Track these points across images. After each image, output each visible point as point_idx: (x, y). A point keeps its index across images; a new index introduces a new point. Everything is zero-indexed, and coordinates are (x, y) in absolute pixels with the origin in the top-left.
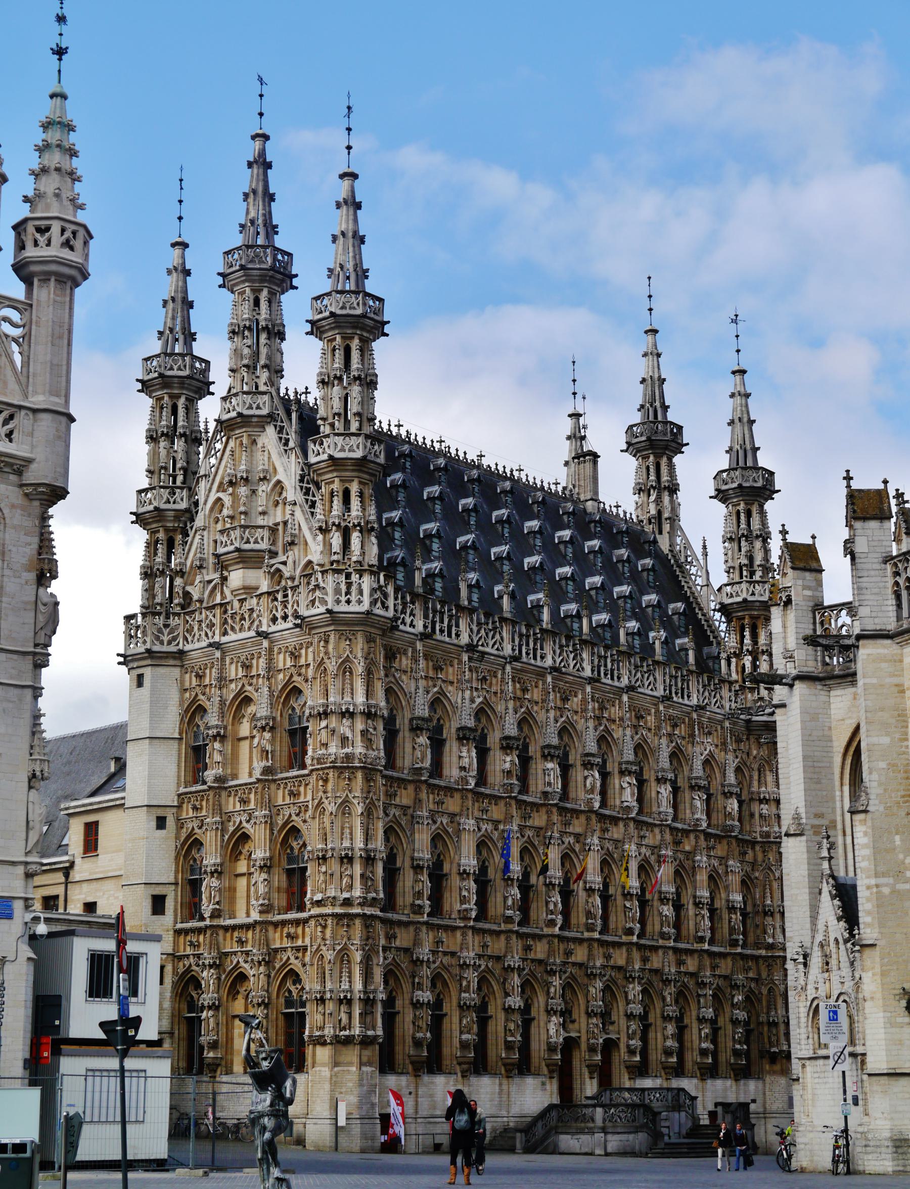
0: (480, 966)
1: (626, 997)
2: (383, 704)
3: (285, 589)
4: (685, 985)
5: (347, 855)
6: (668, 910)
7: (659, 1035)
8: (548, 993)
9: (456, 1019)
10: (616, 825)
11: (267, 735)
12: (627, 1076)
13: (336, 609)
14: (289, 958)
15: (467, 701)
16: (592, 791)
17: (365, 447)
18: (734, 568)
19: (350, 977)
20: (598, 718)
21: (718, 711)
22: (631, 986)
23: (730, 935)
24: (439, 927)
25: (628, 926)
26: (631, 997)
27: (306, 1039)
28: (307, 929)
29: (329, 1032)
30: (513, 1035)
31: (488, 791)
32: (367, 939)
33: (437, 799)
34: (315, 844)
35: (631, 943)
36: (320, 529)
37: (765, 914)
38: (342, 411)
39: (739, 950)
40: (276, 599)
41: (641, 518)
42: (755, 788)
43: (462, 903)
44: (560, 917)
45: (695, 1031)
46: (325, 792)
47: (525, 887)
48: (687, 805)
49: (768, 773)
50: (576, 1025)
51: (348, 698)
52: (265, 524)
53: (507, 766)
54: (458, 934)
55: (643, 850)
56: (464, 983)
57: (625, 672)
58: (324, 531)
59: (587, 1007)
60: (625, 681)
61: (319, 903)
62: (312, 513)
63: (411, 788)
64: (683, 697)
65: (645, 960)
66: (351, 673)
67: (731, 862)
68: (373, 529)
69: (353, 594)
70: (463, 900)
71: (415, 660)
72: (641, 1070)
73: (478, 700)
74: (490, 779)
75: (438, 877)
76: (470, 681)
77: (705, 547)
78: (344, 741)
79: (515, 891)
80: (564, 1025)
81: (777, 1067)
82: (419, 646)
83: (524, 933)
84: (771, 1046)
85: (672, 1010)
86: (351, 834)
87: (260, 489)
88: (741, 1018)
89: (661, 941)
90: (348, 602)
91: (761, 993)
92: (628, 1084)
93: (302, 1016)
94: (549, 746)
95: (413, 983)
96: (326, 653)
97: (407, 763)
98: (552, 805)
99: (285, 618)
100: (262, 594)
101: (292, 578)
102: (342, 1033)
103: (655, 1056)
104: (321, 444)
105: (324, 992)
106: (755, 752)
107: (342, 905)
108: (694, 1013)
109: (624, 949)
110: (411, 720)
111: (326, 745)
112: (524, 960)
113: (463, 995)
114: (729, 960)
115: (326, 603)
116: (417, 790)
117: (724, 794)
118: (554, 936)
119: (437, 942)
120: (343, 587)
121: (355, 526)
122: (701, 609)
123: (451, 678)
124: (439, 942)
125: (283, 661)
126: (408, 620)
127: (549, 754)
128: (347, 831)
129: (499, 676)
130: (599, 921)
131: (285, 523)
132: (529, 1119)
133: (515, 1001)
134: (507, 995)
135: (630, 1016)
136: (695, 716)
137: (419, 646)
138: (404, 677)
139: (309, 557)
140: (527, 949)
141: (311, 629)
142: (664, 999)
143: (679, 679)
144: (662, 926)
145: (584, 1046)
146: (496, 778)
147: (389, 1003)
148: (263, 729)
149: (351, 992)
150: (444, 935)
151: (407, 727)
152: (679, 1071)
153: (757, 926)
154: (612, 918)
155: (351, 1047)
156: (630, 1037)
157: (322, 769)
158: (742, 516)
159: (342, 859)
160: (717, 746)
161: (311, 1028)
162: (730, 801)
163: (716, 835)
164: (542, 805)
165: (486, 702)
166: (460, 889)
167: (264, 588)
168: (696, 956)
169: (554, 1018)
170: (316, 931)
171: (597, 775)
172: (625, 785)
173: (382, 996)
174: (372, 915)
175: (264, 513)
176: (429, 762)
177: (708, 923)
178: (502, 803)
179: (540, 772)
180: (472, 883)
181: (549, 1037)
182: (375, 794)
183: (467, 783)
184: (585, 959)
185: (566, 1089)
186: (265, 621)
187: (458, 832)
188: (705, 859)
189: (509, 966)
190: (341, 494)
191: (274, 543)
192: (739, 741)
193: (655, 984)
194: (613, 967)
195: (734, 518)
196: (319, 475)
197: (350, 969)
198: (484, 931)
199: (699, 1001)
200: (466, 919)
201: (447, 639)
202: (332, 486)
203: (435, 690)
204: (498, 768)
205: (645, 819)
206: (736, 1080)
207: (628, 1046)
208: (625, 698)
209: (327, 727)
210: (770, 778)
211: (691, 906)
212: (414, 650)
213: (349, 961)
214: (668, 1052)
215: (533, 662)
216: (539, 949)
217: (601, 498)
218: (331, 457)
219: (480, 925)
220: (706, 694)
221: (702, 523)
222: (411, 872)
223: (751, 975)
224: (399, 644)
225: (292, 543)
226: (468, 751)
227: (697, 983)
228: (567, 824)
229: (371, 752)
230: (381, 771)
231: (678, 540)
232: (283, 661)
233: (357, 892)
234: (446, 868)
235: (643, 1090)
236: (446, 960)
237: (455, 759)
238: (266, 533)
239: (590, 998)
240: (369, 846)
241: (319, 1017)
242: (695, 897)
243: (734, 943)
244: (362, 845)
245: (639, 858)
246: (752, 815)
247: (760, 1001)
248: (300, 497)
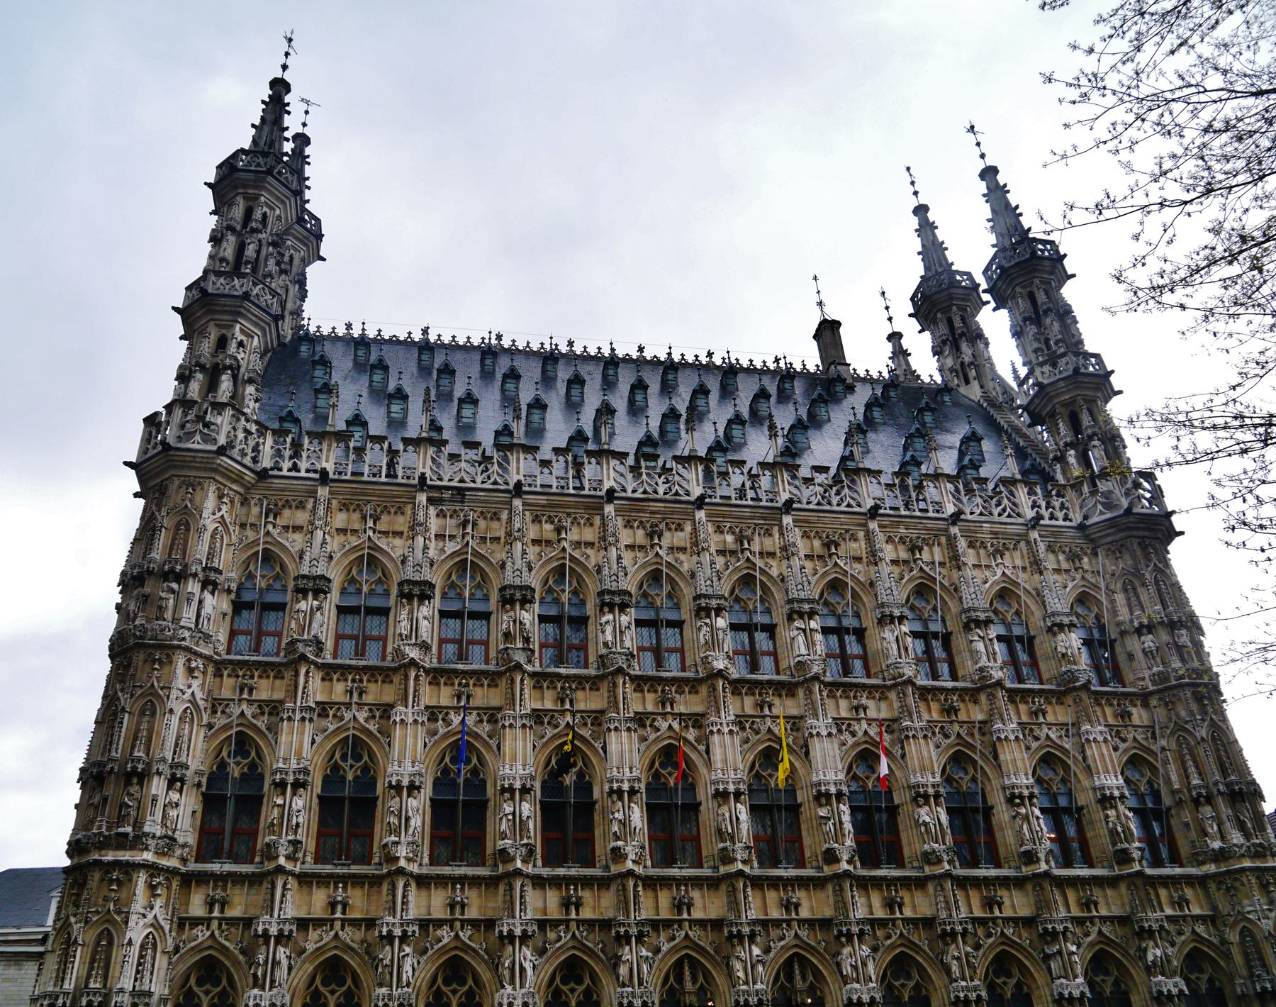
1: (841, 973)
10: (793, 695)
22: (847, 950)
23: (1114, 844)
37: (1196, 802)
39: (1137, 867)
89: (927, 869)
91: (1224, 942)
142: (948, 970)
153: (1187, 825)
168: (1029, 887)
174: (117, 864)
246: (1131, 656)
247: (1228, 956)
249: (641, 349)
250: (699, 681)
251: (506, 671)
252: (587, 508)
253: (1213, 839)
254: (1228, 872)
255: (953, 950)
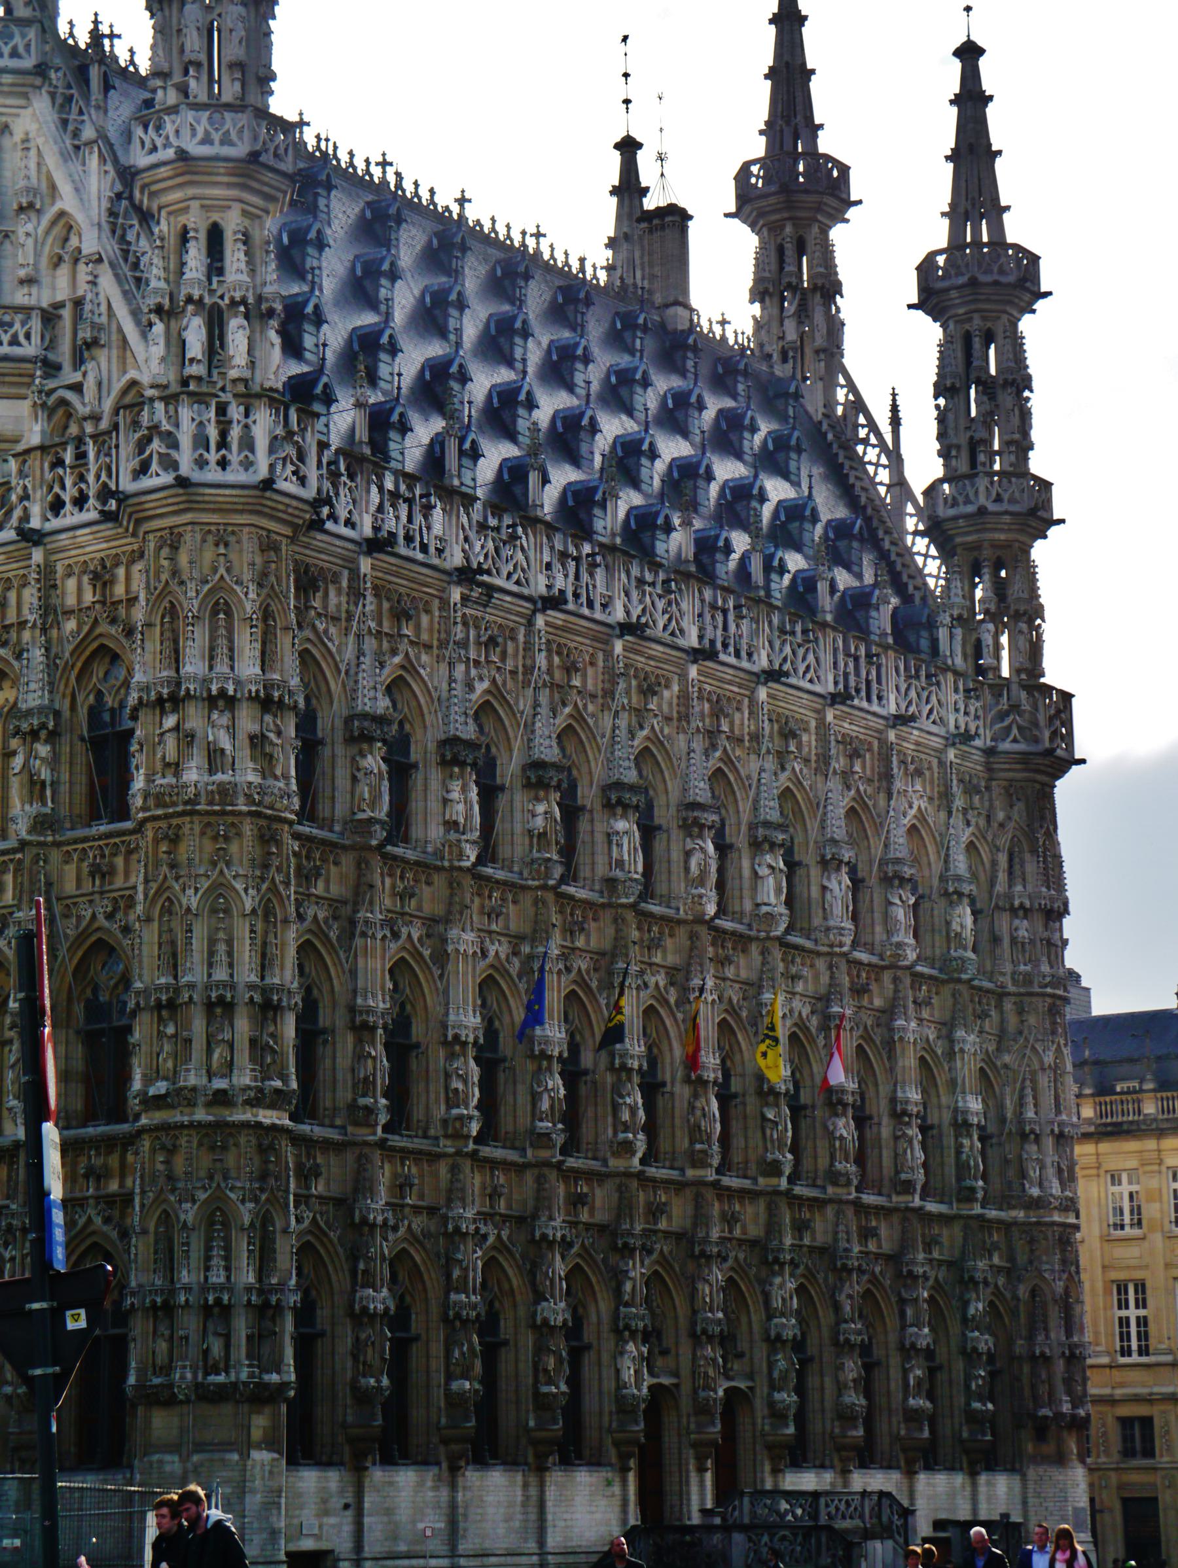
0: (485, 1237)
2: (295, 682)
3: (80, 441)
4: (874, 1280)
5: (221, 998)
6: (845, 1127)
7: (828, 1381)
8: (618, 1291)
9: (437, 1349)
11: (43, 750)
12: (767, 1468)
13: (197, 476)
14: (90, 1220)
15: (459, 689)
16: (701, 881)
17: (255, 138)
18: (958, 447)
19: (227, 1258)
20: (712, 735)
21: (934, 729)
22: (778, 1280)
23: (959, 1179)
24: (405, 1153)
25: (770, 1157)
26: (777, 1303)
27: (129, 1391)
28: (130, 1158)
29: (184, 1375)
30: (550, 1382)
31: (500, 875)
32: (263, 1176)
33: (400, 886)
34: (148, 975)
35: (777, 1193)
36: (159, 310)
37: (1024, 1136)
38: (203, 57)
39: (977, 1210)
40: (60, 463)
41: (768, 349)
42: (1001, 887)
43: (449, 1107)
44: (641, 1136)
45: (895, 1374)
46: (173, 866)
47: (573, 1075)
48: (878, 916)
49: (1027, 856)
50: (670, 1361)
51: (222, 668)
52: (33, 302)
53: (539, 822)
54: (443, 1169)
55: (797, 1004)
56: (456, 1273)
57: (762, 643)
58: (167, 313)
59: (693, 1324)
60: (762, 661)
61: (159, 1102)
62: (138, 280)
63: (348, 861)
64: (869, 700)
65: (800, 1227)
66: (229, 614)
67: (960, 1033)
68: (271, 313)
69: (235, 447)
70: (453, 1099)
71: (356, 594)
72: (797, 1455)
73: (481, 687)
74: (504, 851)
75: (401, 1048)
76: (464, 644)
77: (895, 409)
78: (215, 758)
79: (556, 1083)
80: (649, 1361)
81: (1049, 1448)
82: (365, 565)
83: (572, 1170)
84: (1038, 1405)
85: (854, 1329)
86: (230, 954)
87: (21, 231)
88: (982, 1348)
89: (830, 1190)
90: (223, 464)
92: (768, 1486)
93: (120, 1346)
94: (618, 785)
95: (354, 1272)
96: (175, 573)
97: (341, 810)
98: (623, 906)
99: (80, 501)
100: (28, 452)
101: (96, 418)
102: (212, 1378)
103: (821, 1424)
104: (158, 128)
105: (173, 1292)
106: (1001, 816)
107: (209, 1105)
108: (893, 1338)
109: (762, 1204)
110: (349, 720)
111: (176, 768)
112: (573, 1224)
113: (453, 1297)
114: (957, 1229)
115: (175, 466)
116: (361, 865)
117: (946, 894)
118: (628, 1175)
119: (401, 1186)
120: (213, 433)
121: (234, 303)
122: (888, 532)
123: (425, 637)
124: (401, 1186)
125: (74, 591)
126: (343, 514)
127: (619, 802)
128: (222, 948)
129: (521, 638)
130: (716, 1147)
131: (78, 303)
132: (594, 1559)
133: (556, 1311)
134: (539, 1297)
135: (775, 1342)
136: (892, 736)
137: (365, 565)
138: (332, 630)
139: (132, 374)
140: (577, 1201)
141: (138, 522)
142: (837, 1307)
143: (862, 660)
144: (833, 1158)
145: (685, 1403)
146: (514, 847)
147: (305, 1314)
148: (34, 734)
149: (231, 1290)
150: (414, 1170)
151: (339, 736)
152: (867, 1457)
153: (1007, 1161)
154: (738, 1142)
155: (227, 1409)
156: (773, 1387)
157: (167, 817)
158: (977, 343)
159: (210, 1006)
160: (931, 799)
161: (142, 1372)
162: (959, 910)
163: (931, 977)
164: (603, 905)
165: (496, 690)
166: (447, 1076)
167: (36, 440)
168: (896, 1219)
169: (631, 1347)
170: (153, 1161)
171: (711, 848)
172: (763, 871)
173: (294, 1299)
174: (274, 1127)
175: (29, 281)
176: (386, 807)
177: (920, 1155)
178: (527, 900)
179: (600, 838)
180: (472, 1063)
181: (620, 1385)
182: (279, 870)
183: (461, 855)
184: (688, 1223)
185: (654, 1497)
186: (36, 510)
187: (441, 958)
188: (913, 1024)
189: (544, 1236)
190: (203, 236)
191: (51, 346)
192: (971, 790)
193: (820, 1277)
194: (741, 1242)
195: (959, 346)
196: (153, 195)
197: (227, 1240)
198: (493, 1164)
199: (903, 1314)
200: (459, 1136)
201: (420, 556)
202: (182, 219)
203: (397, 660)
204: (518, 828)
205: (800, 941)
206: (973, 1474)
207: (771, 1404)
208: (762, 693)
209: (177, 728)
210: (1031, 867)
211: (885, 1120)
212: (355, 573)
213: (226, 1225)
214: (846, 1416)
215: (586, 611)
216: (598, 1203)
217: (694, 302)
218: (182, 155)
219: (486, 1151)
220: (913, 694)
221: (890, 355)
222: (350, 1038)
223: (996, 1260)
224: (322, 561)
225: (93, 344)
226: (464, 789)
227: (898, 1275)
228: (653, 945)
229: (270, 782)
230: (291, 823)
231: (841, 394)
232: (74, 591)
233: (244, 1078)
234: (417, 1031)
235: (816, 1495)
236: (418, 1223)
237: (434, 805)
238: (36, 324)
239: (699, 1304)
240: (268, 981)
241: (163, 1346)
242: (893, 1100)
243: (968, 1195)
244: (254, 978)
245: (789, 1023)
246: (996, 940)
247: (1014, 1313)
248: (111, 248)
249: (462, 201)
250: (680, 922)
251: (538, 888)
252: (595, 639)
253: (1032, 1184)
254: (1038, 1223)
255: (847, 1289)
